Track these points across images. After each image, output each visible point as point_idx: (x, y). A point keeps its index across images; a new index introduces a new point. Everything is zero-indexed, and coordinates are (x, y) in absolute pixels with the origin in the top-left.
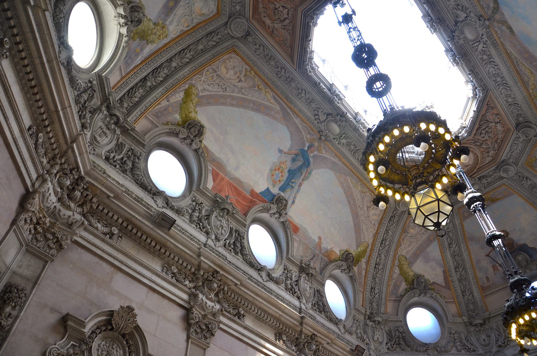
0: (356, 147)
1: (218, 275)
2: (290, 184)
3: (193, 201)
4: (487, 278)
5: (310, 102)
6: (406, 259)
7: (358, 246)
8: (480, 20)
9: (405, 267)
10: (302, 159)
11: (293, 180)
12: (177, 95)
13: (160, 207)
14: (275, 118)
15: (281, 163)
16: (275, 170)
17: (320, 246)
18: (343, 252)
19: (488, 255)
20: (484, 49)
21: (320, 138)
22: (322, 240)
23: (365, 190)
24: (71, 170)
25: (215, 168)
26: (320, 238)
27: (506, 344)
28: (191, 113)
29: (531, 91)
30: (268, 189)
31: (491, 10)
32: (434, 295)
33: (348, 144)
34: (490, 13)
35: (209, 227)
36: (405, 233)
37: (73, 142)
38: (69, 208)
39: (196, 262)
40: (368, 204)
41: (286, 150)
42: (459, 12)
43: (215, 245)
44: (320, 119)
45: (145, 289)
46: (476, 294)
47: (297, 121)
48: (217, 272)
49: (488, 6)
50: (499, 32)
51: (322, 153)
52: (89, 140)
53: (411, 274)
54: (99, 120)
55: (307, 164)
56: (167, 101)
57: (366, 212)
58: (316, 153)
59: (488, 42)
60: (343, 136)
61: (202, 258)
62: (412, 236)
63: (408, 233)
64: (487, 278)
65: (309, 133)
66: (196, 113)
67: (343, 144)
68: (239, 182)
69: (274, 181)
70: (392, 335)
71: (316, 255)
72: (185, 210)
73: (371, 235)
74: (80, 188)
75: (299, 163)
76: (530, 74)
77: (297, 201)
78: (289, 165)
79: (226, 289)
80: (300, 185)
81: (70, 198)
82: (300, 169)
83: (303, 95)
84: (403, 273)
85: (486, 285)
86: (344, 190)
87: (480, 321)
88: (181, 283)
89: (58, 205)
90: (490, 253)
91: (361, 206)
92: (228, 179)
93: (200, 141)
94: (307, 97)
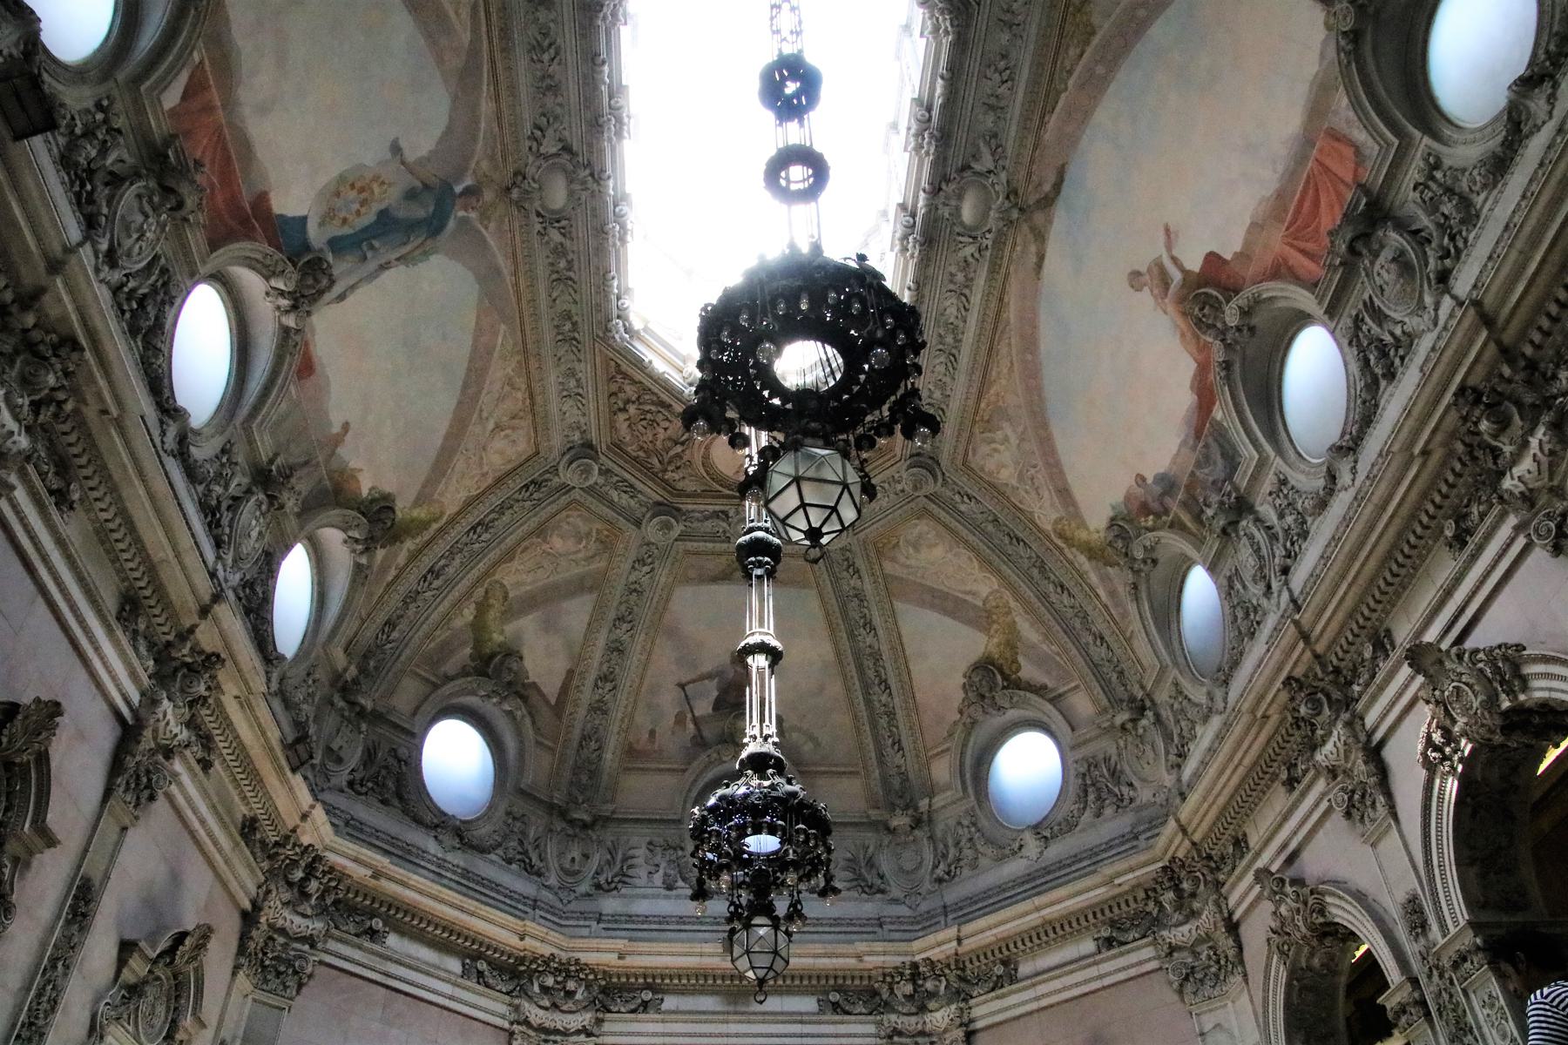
0: (569, 269)
1: (75, 356)
2: (364, 246)
3: (99, 106)
4: (652, 733)
5: (549, 88)
6: (506, 597)
7: (417, 503)
8: (1008, 197)
9: (492, 615)
10: (431, 209)
11: (376, 243)
14: (440, 61)
15: (376, 178)
16: (353, 186)
17: (336, 446)
19: (682, 686)
20: (970, 259)
21: (508, 189)
22: (348, 437)
23: (521, 382)
26: (346, 427)
27: (613, 885)
29: (983, 405)
30: (304, 219)
31: (1037, 196)
32: (519, 713)
33: (559, 251)
34: (1031, 200)
35: (105, 210)
36: (538, 537)
40: (505, 419)
41: (410, 156)
42: (985, 150)
44: (540, 144)
46: (608, 756)
47: (486, 107)
49: (1040, 185)
50: (1018, 248)
51: (486, 228)
53: (497, 638)
55: (434, 226)
57: (488, 433)
58: (473, 215)
59: (988, 253)
60: (564, 223)
62: (549, 554)
63: (545, 540)
64: (652, 733)
65: (492, 158)
67: (547, 243)
73: (463, 495)
75: (420, 213)
76: (1005, 371)
77: (351, 299)
78: (389, 197)
79: (69, 407)
80: (384, 267)
82: (411, 227)
83: (546, 57)
84: (478, 626)
85: (639, 747)
86: (475, 348)
87: (586, 817)
90: (689, 683)
91: (485, 414)
94: (551, 69)
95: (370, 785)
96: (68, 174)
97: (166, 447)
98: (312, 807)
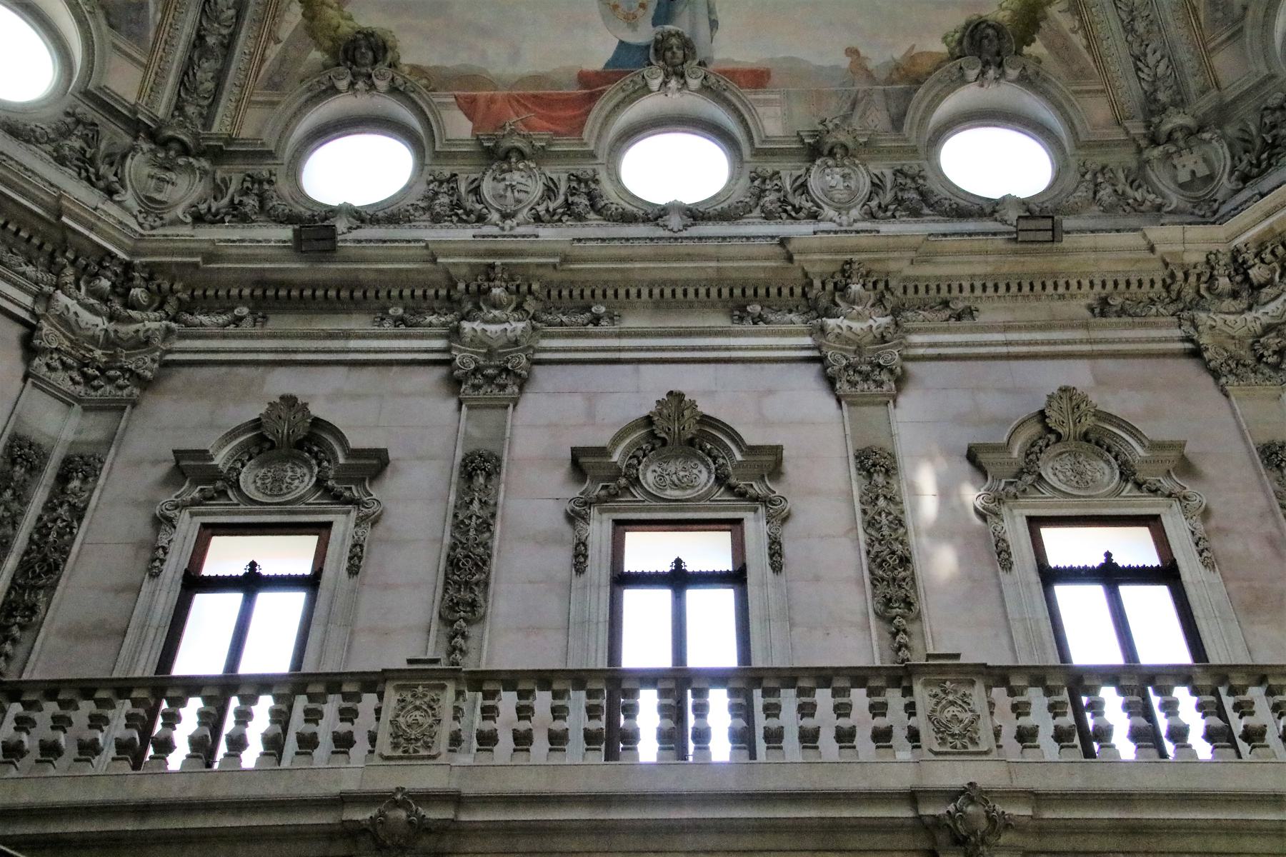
12: (288, 17)
13: (343, 233)
18: (957, 36)
22: (862, 52)
24: (100, 264)
25: (460, 93)
26: (852, 52)
28: (338, 27)
30: (621, 43)
37: (59, 217)
38: (131, 320)
39: (439, 277)
43: (503, 229)
45: (342, 370)
48: (492, 266)
52: (139, 208)
54: (138, 167)
56: (276, 43)
61: (439, 260)
66: (350, 19)
68: (537, 79)
69: (626, 18)
70: (1251, 135)
71: (860, 96)
72: (409, 208)
74: (137, 282)
77: (721, 16)
81: (131, 304)
88: (417, 325)
89: (112, 326)
92: (506, 92)
93: (390, 66)
95: (1265, 156)
96: (445, 221)
97: (675, 229)
98: (1145, 236)
